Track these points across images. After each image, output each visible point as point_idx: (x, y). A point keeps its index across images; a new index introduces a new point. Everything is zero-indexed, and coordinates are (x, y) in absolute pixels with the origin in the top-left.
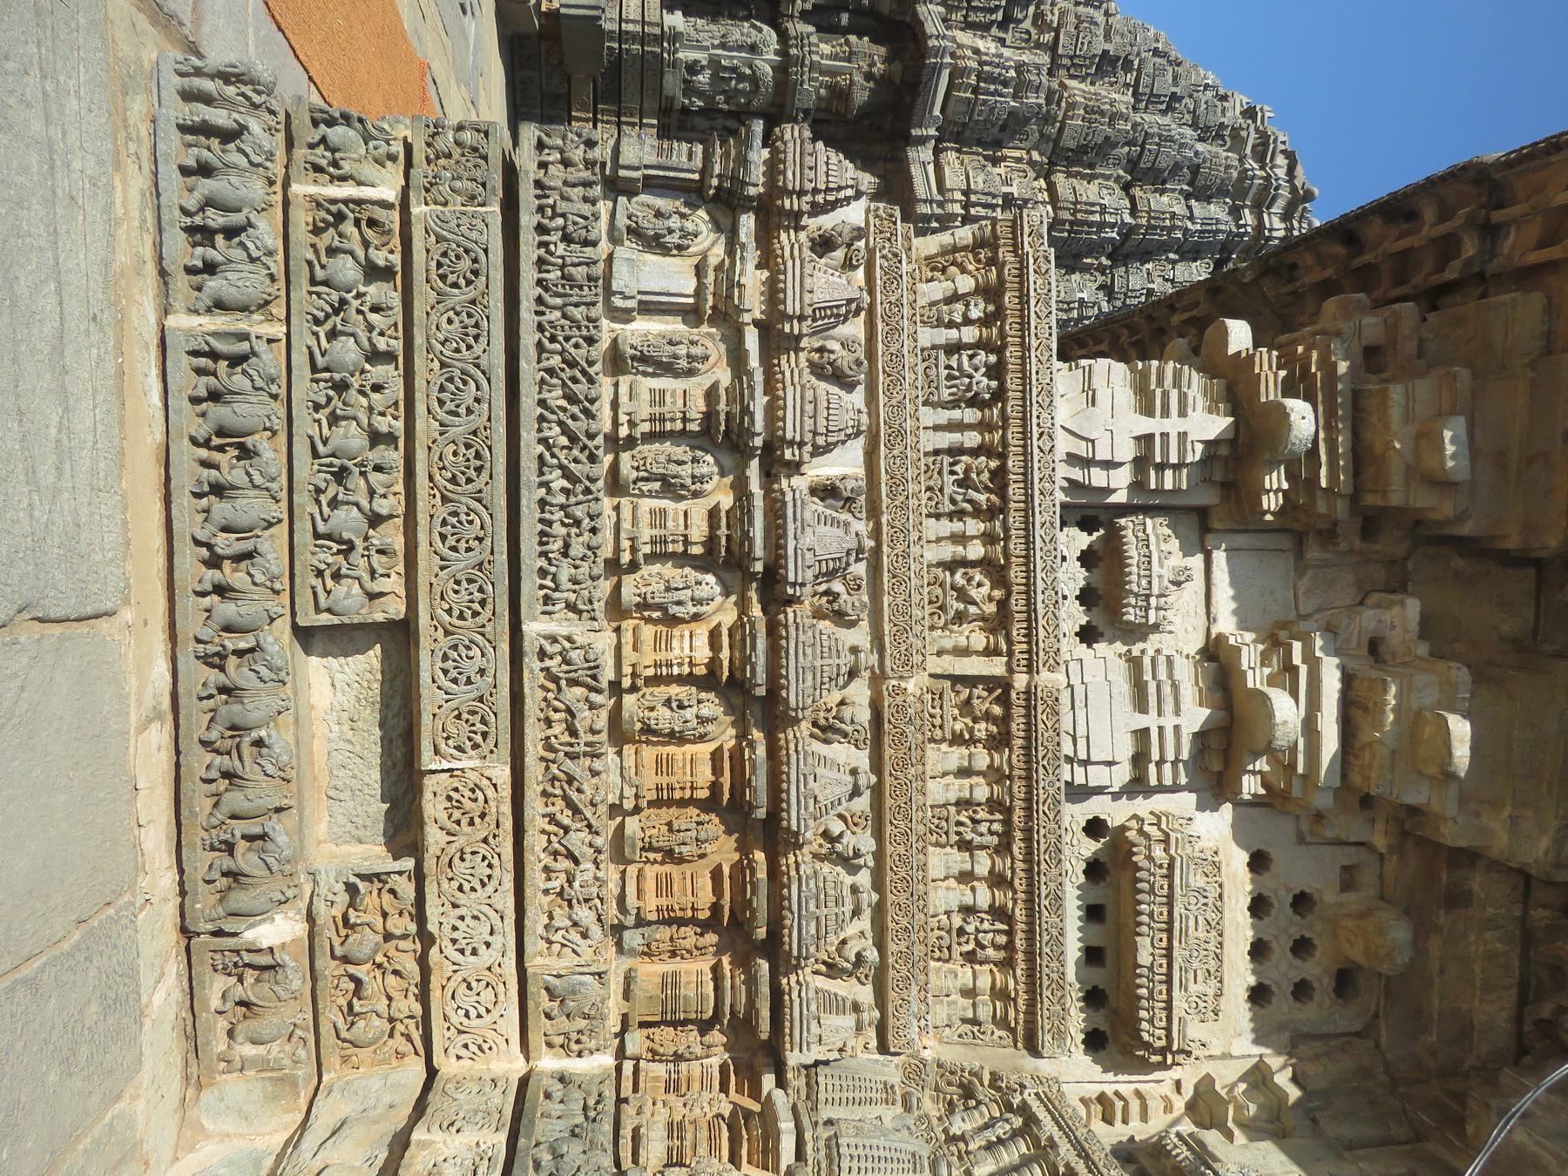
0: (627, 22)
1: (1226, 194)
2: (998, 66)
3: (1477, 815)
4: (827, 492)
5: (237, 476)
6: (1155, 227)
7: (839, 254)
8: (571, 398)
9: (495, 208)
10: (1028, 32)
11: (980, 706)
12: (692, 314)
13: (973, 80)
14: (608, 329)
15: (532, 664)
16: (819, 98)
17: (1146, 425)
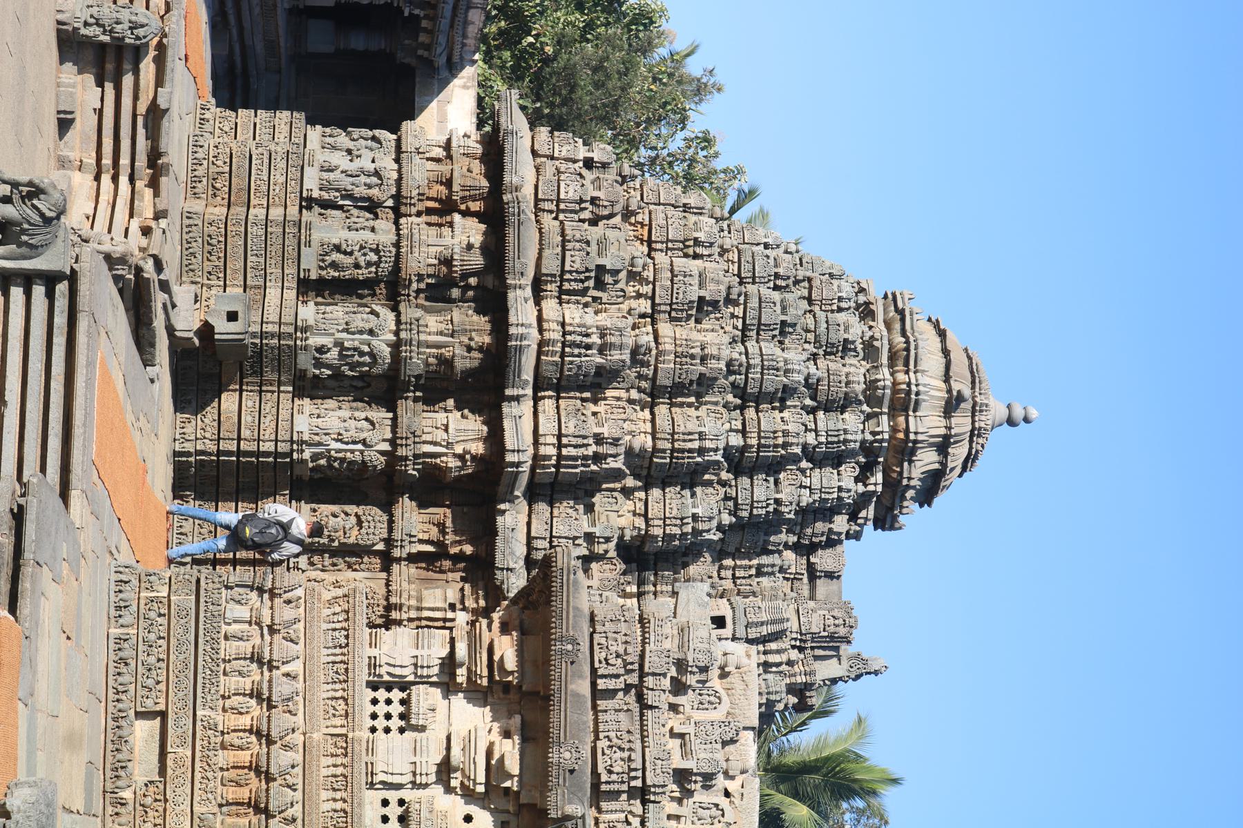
0: (267, 323)
1: (860, 403)
2: (580, 334)
3: (530, 791)
4: (287, 675)
5: (124, 670)
6: (765, 446)
7: (294, 604)
8: (213, 649)
9: (194, 597)
10: (622, 290)
11: (339, 744)
12: (250, 623)
13: (558, 348)
14: (224, 628)
15: (199, 723)
16: (427, 364)
17: (416, 653)
